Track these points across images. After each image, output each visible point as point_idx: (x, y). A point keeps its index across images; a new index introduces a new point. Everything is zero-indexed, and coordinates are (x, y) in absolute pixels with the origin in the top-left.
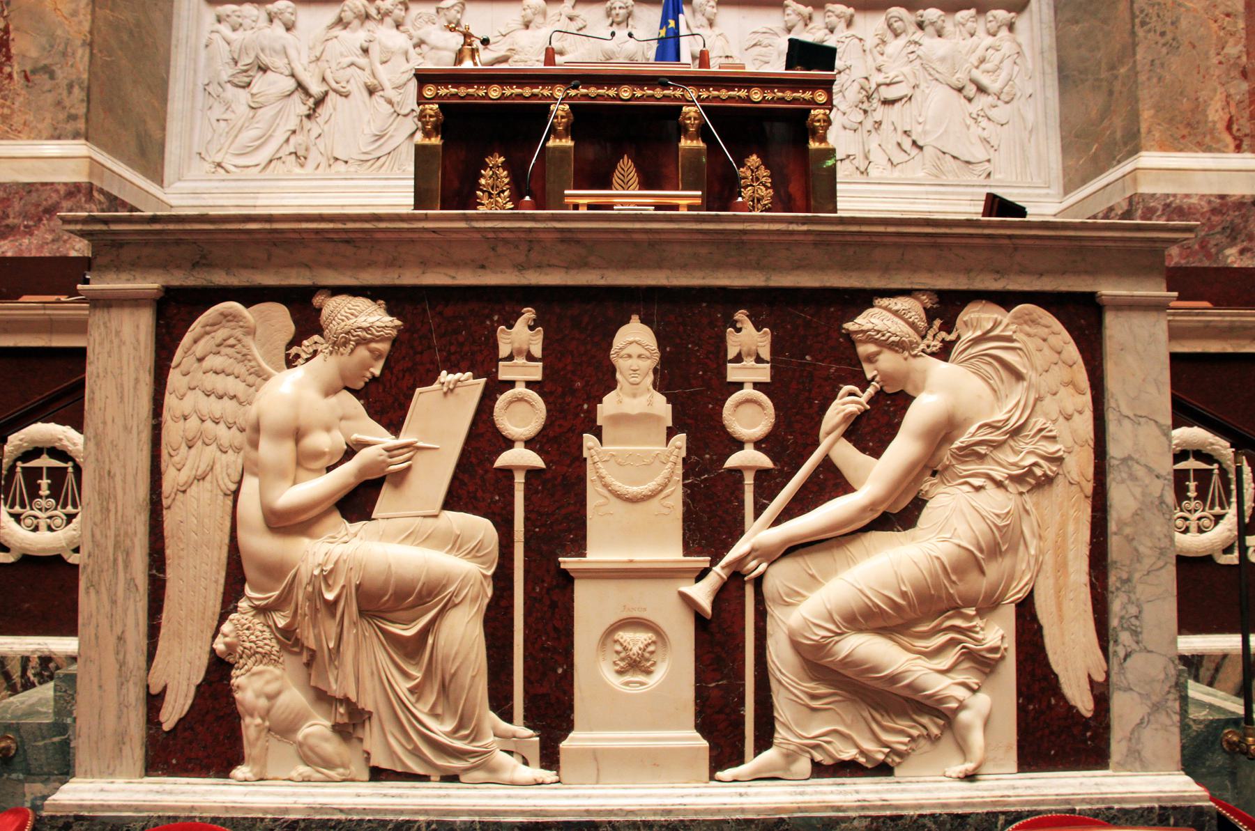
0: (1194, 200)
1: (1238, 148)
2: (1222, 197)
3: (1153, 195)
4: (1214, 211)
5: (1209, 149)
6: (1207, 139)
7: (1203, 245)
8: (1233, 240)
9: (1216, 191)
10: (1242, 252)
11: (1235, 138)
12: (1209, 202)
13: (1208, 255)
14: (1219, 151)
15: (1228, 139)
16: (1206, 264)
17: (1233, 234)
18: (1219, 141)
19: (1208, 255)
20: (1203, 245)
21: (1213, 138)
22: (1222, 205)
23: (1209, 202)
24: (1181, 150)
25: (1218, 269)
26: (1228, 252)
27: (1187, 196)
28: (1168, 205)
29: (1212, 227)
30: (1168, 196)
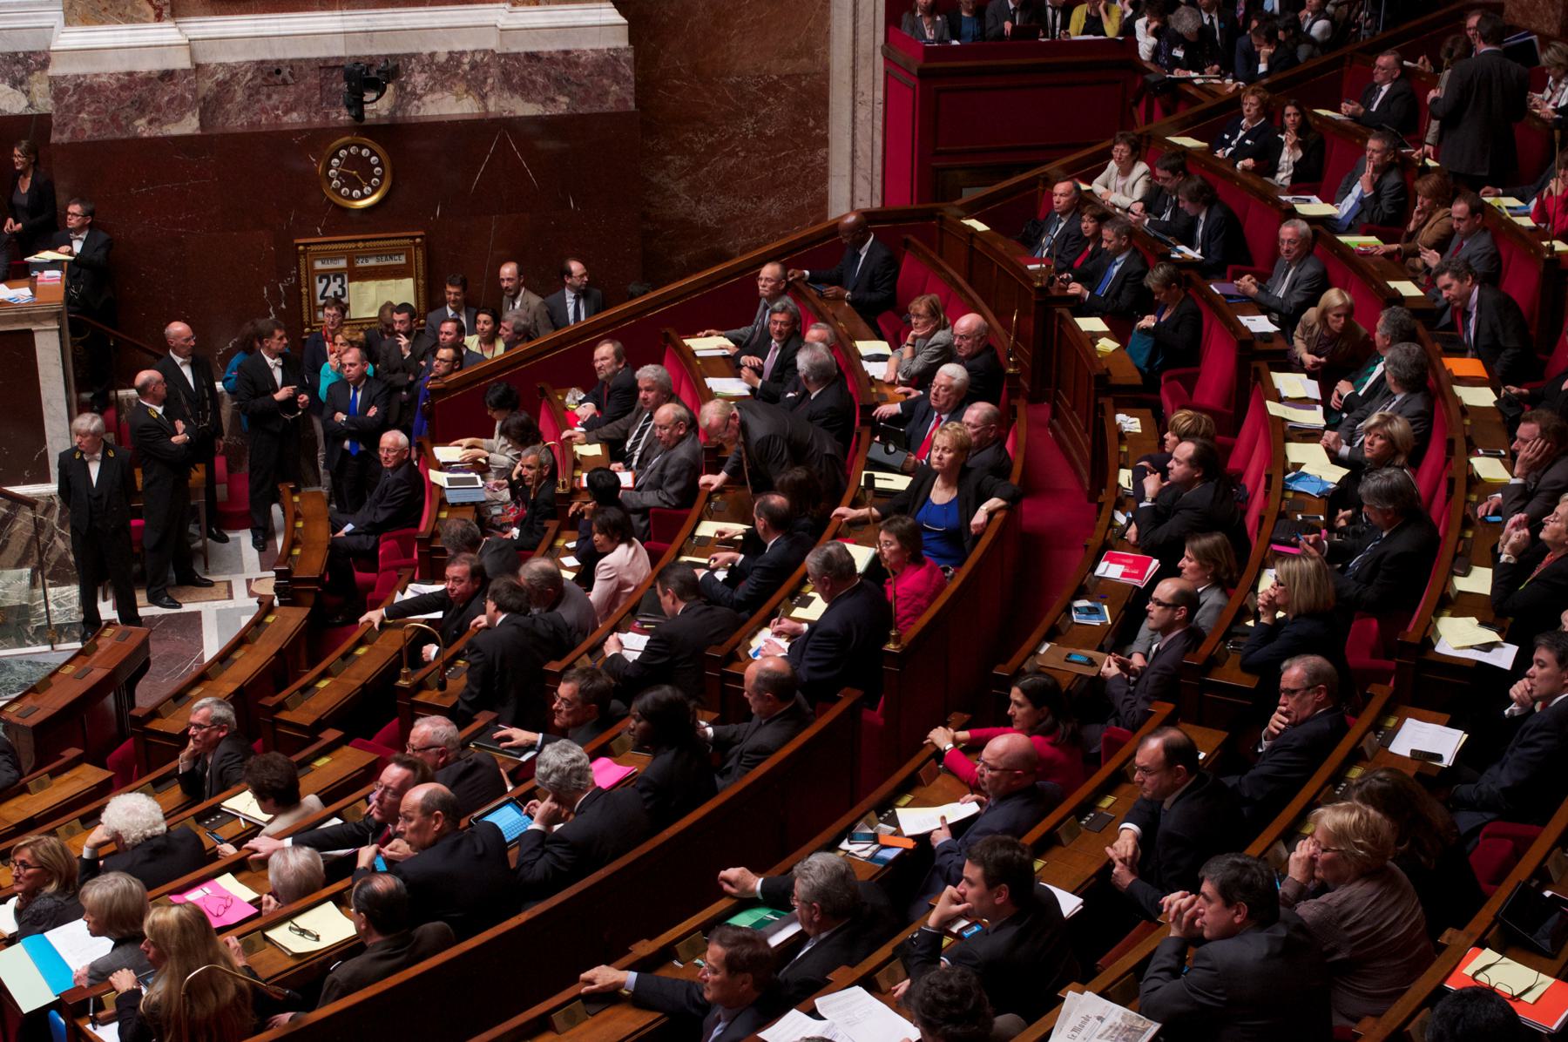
0: (104, 79)
1: (159, 18)
2: (130, 74)
3: (64, 77)
4: (123, 87)
5: (130, 20)
6: (129, 10)
7: (114, 119)
8: (141, 112)
9: (125, 67)
10: (150, 122)
11: (155, 8)
12: (118, 80)
13: (119, 127)
14: (140, 21)
15: (149, 9)
16: (118, 135)
17: (141, 107)
18: (139, 11)
19: (119, 127)
20: (114, 119)
21: (134, 8)
22: (131, 81)
23: (118, 80)
24: (103, 23)
25: (124, 141)
26: (138, 123)
27: (97, 75)
28: (78, 86)
29: (122, 101)
30: (78, 76)
